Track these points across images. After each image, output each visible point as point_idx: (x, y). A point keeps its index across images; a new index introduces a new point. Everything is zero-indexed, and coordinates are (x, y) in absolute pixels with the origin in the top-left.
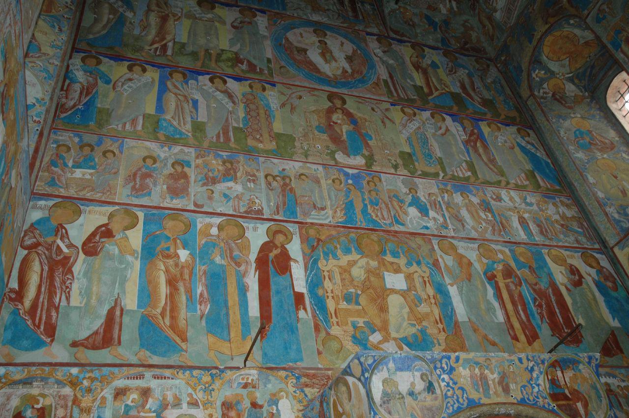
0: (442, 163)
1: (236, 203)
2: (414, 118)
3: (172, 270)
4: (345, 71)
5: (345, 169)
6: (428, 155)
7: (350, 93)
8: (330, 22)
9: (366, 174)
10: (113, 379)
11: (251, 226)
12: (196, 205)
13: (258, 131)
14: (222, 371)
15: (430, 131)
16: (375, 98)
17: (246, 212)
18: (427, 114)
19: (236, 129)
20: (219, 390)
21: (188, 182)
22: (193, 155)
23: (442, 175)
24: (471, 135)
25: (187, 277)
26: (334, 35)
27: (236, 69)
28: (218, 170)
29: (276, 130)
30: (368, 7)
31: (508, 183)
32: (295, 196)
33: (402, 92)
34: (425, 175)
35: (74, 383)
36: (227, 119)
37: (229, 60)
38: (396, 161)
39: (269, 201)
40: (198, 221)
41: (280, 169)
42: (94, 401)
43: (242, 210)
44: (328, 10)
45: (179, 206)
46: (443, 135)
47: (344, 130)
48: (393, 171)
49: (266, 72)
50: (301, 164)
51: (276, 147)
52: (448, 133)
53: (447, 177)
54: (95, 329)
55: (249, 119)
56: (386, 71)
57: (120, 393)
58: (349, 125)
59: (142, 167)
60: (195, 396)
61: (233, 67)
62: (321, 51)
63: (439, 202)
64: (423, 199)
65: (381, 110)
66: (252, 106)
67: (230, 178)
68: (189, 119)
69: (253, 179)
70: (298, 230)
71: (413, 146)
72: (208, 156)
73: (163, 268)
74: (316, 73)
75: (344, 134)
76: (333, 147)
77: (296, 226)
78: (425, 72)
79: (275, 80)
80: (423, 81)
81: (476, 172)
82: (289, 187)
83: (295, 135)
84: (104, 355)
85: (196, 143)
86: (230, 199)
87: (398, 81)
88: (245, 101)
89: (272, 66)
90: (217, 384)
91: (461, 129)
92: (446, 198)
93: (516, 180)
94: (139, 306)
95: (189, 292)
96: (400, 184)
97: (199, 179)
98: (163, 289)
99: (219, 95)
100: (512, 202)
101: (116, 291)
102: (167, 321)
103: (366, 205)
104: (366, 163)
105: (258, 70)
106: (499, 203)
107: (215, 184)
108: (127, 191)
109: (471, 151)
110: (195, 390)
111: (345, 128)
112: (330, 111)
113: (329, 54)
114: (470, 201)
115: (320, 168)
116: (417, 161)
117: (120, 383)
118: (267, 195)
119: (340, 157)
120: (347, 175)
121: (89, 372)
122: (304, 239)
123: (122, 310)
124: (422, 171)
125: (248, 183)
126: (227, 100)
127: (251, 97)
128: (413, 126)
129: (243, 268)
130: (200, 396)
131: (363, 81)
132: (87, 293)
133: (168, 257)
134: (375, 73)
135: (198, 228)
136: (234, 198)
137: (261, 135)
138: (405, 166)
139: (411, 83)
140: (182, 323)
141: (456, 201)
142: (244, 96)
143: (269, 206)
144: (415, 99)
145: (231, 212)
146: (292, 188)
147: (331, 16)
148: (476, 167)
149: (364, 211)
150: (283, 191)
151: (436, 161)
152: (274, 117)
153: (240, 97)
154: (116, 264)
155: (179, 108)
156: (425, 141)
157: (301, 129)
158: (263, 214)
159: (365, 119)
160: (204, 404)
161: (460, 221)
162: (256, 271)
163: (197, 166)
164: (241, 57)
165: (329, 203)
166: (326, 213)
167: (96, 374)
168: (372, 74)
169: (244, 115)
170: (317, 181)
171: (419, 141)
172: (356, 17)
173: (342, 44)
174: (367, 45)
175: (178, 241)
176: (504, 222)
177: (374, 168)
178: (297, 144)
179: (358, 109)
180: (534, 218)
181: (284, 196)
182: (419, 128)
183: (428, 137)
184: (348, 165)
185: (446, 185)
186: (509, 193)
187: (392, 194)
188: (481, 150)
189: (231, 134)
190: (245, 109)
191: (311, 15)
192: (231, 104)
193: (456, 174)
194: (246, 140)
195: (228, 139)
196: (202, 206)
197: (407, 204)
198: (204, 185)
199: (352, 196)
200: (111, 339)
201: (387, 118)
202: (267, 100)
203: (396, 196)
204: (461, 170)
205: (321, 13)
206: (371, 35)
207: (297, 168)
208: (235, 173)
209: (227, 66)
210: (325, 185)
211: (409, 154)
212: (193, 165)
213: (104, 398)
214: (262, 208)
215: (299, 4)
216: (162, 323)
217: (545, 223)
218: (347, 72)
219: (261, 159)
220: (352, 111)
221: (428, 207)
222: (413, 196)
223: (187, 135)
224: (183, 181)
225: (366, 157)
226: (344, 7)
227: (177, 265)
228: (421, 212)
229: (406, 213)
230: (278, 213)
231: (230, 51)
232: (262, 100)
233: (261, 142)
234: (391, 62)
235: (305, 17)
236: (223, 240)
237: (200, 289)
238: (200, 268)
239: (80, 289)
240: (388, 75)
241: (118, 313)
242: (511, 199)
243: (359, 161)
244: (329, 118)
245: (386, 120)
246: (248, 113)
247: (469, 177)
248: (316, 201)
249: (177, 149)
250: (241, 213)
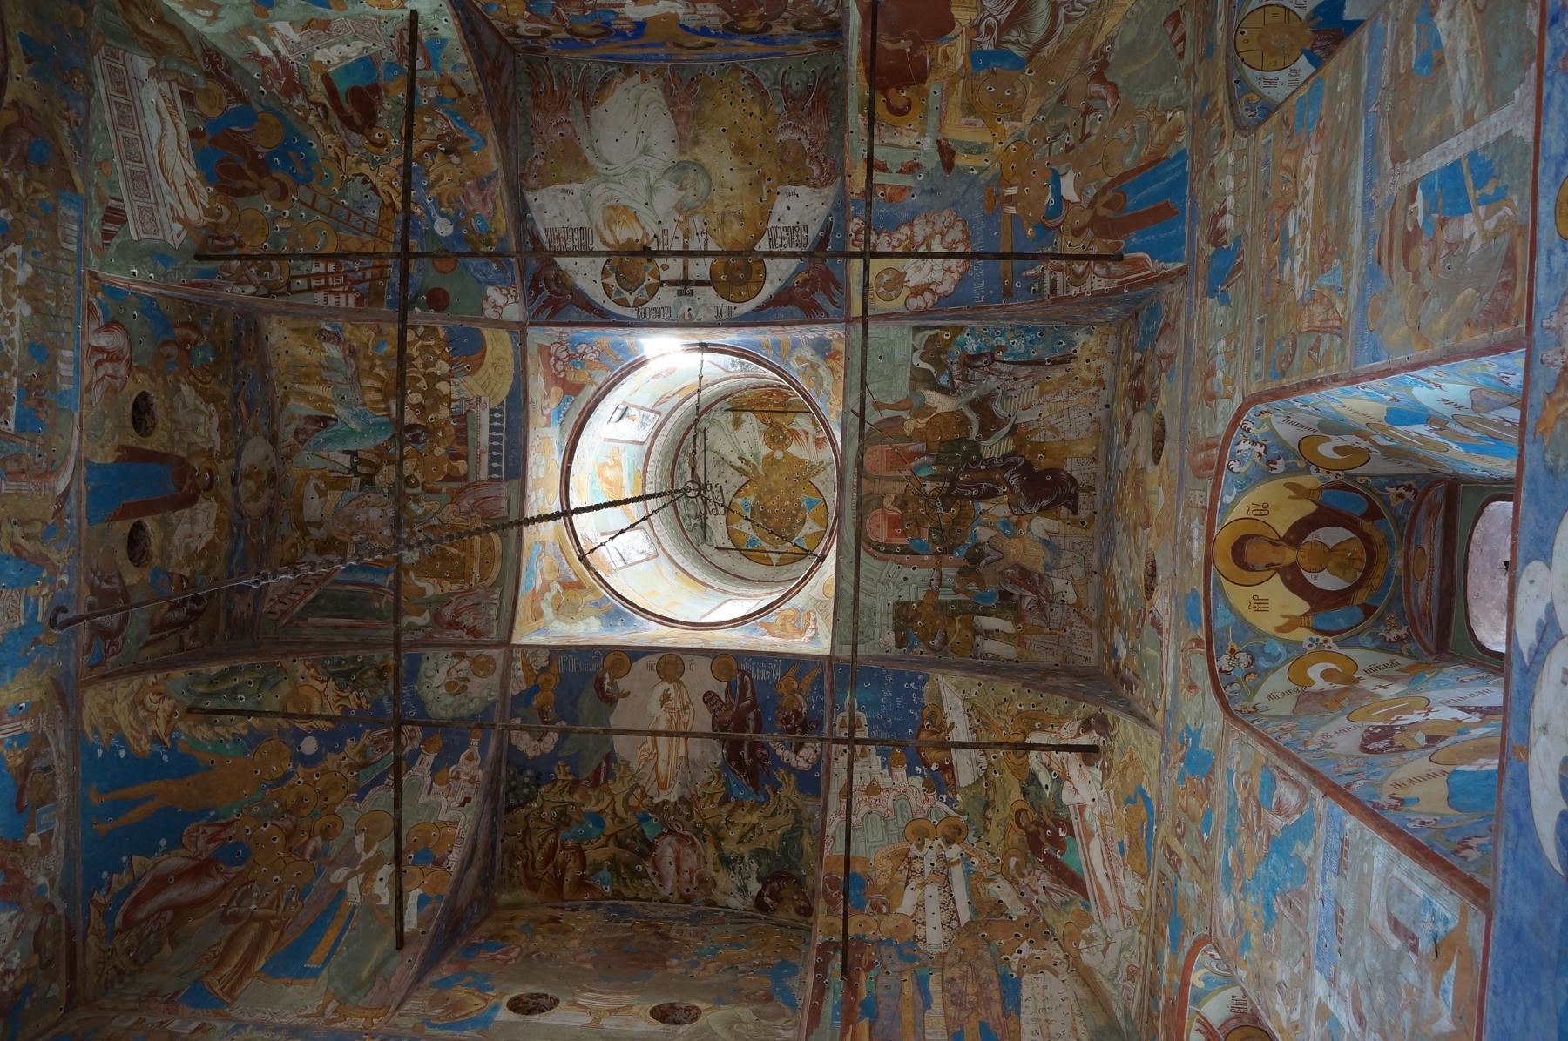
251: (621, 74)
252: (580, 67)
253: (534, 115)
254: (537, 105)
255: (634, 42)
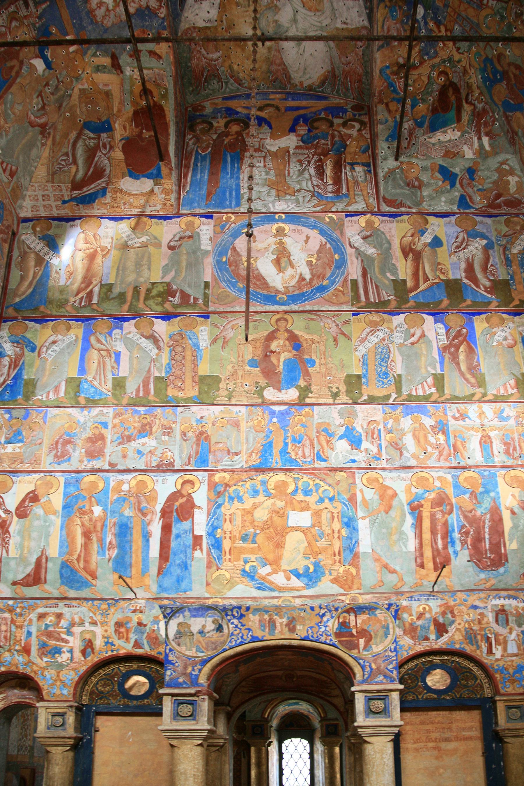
0: (400, 381)
1: (149, 458)
2: (380, 328)
3: (87, 524)
4: (302, 279)
5: (272, 407)
6: (384, 375)
7: (301, 309)
8: (297, 209)
9: (296, 409)
10: (38, 607)
11: (160, 479)
12: (111, 465)
13: (180, 378)
14: (117, 601)
15: (398, 339)
16: (333, 309)
17: (158, 466)
18: (398, 320)
19: (157, 379)
20: (113, 614)
21: (105, 444)
22: (111, 415)
23: (394, 396)
24: (455, 338)
25: (99, 529)
26: (300, 227)
27: (167, 306)
28: (135, 428)
29: (201, 373)
30: (358, 169)
31: (484, 395)
32: (210, 444)
33: (373, 293)
34: (372, 400)
35: (11, 610)
36: (150, 368)
37: (159, 295)
38: (338, 388)
39: (181, 452)
40: (111, 479)
41: (199, 417)
42: (25, 621)
43: (154, 464)
44: (299, 190)
45: (95, 468)
46: (413, 344)
47: (282, 359)
48: (331, 401)
49: (201, 301)
50: (222, 408)
51: (197, 393)
52: (421, 341)
53: (400, 399)
54: (28, 572)
55: (173, 365)
56: (359, 266)
57: (41, 617)
58: (290, 352)
59: (63, 434)
60: (95, 618)
61: (162, 304)
62: (275, 256)
63: (379, 430)
64: (359, 429)
65: (337, 326)
66: (179, 349)
67: (144, 434)
68: (110, 376)
69: (168, 430)
70: (207, 478)
71: (367, 365)
72: (126, 414)
73: (79, 523)
74: (263, 289)
75: (281, 364)
76: (263, 382)
77: (206, 474)
78: (417, 256)
79: (211, 309)
80: (410, 271)
81: (443, 387)
82: (205, 435)
83: (222, 374)
84: (33, 591)
85: (116, 402)
86: (144, 454)
87: (373, 278)
88: (171, 343)
89: (209, 292)
90: (112, 610)
91: (442, 331)
92: (389, 426)
93: (498, 391)
94: (60, 554)
95: (101, 541)
96: (336, 416)
97: (115, 438)
98: (79, 540)
99: (145, 343)
100: (480, 419)
101: (42, 544)
102: (82, 564)
103: (286, 445)
104: (299, 397)
105: (192, 301)
106: (461, 422)
107: (130, 441)
108: (51, 458)
109: (446, 360)
110: (95, 614)
111: (284, 357)
112: (271, 337)
113: (286, 259)
114: (421, 424)
115: (243, 409)
116: (367, 384)
117: (42, 610)
118: (181, 446)
119: (270, 394)
120: (273, 413)
121: (20, 603)
122: (212, 486)
123: (47, 558)
124: (368, 396)
125: (163, 437)
126: (152, 346)
127: (178, 338)
128: (374, 339)
129: (148, 517)
130: (98, 618)
131: (322, 289)
132: (21, 547)
133: (84, 513)
134: (343, 273)
135: (111, 486)
136: (147, 453)
137: (183, 382)
138: (349, 392)
139: (392, 278)
140: (93, 566)
141: (402, 426)
142: (171, 338)
143: (181, 457)
144: (389, 301)
145: (143, 468)
146: (208, 436)
147: (301, 199)
148: (446, 379)
149: (284, 452)
150: (198, 440)
151: (393, 380)
152: (201, 357)
153: (166, 338)
154: (42, 522)
155: (102, 365)
156: (385, 357)
157: (230, 367)
158: (174, 466)
159: (313, 341)
160: (102, 623)
161: (399, 449)
162: (160, 519)
163: (114, 426)
164: (174, 287)
165: (245, 447)
166: (240, 457)
167: (25, 604)
168: (337, 276)
169: (168, 361)
170: (237, 425)
171: (377, 357)
172: (338, 191)
173: (308, 238)
174: (342, 233)
175: (93, 499)
176: (459, 444)
177: (308, 401)
178: (222, 385)
179: (307, 328)
180: (503, 435)
181: (198, 445)
182: (384, 339)
183: (392, 349)
184: (278, 401)
185: (394, 409)
186: (481, 408)
187: (322, 429)
188: (462, 357)
189: (152, 386)
190: (171, 353)
191: (273, 203)
192: (157, 351)
193: (414, 393)
194: (166, 390)
195: (147, 391)
196: (116, 465)
197: (337, 437)
198: (120, 444)
199: (273, 437)
200: (40, 578)
201: (343, 334)
202: (197, 338)
203: (326, 430)
204: (423, 387)
205: (288, 197)
206: (352, 216)
207: (217, 413)
208: (151, 427)
209: (157, 304)
210: (245, 428)
211: (359, 377)
212: (110, 425)
213: (31, 620)
214: (174, 461)
215: (260, 192)
216: (77, 566)
217: (516, 439)
218: (304, 279)
219: (180, 409)
220: (297, 333)
221: (363, 437)
222: (347, 427)
223: (107, 395)
224: (100, 443)
225: (301, 388)
226: (322, 180)
227: (91, 520)
228: (352, 446)
229: (332, 448)
230: (189, 463)
231: (162, 283)
232: (190, 339)
233: (183, 390)
234: (371, 251)
235: (264, 210)
236: (132, 495)
237: (109, 538)
238: (111, 520)
239: (16, 544)
240: (360, 272)
241: (44, 560)
242: (481, 415)
243: (292, 394)
244: (267, 346)
245: (341, 338)
246: (173, 358)
247: (431, 394)
248: (231, 447)
249: (96, 411)
250: (152, 467)
251: (314, 86)
252: (337, 92)
253: (361, 71)
254: (360, 76)
255: (301, 112)
